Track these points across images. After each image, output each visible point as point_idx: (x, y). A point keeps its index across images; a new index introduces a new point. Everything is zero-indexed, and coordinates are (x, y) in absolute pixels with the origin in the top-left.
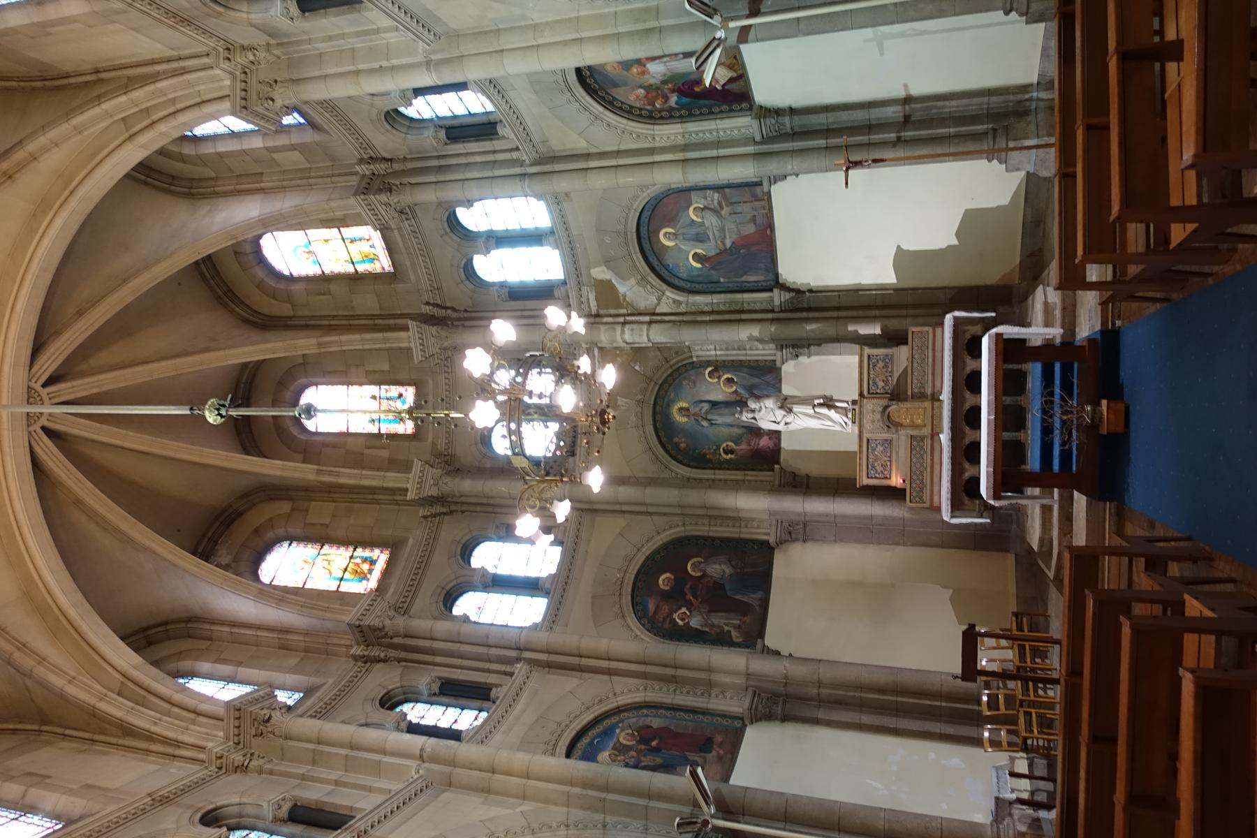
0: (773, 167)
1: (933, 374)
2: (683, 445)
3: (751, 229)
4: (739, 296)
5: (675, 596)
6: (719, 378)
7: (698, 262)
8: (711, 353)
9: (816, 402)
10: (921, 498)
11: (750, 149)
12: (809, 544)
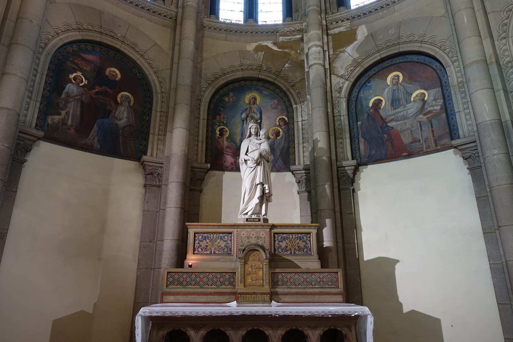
1: (297, 294)
2: (227, 99)
3: (406, 139)
4: (348, 135)
5: (98, 77)
6: (280, 126)
7: (374, 104)
9: (266, 186)
10: (172, 283)
12: (141, 190)
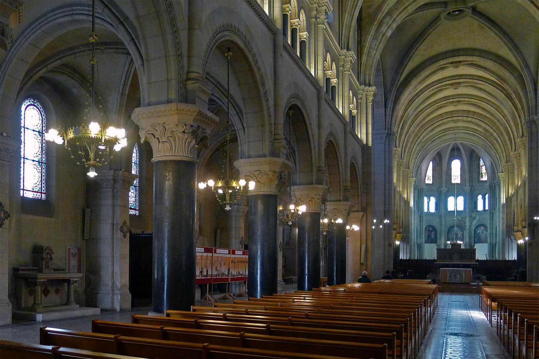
5: (429, 231)
8: (465, 233)
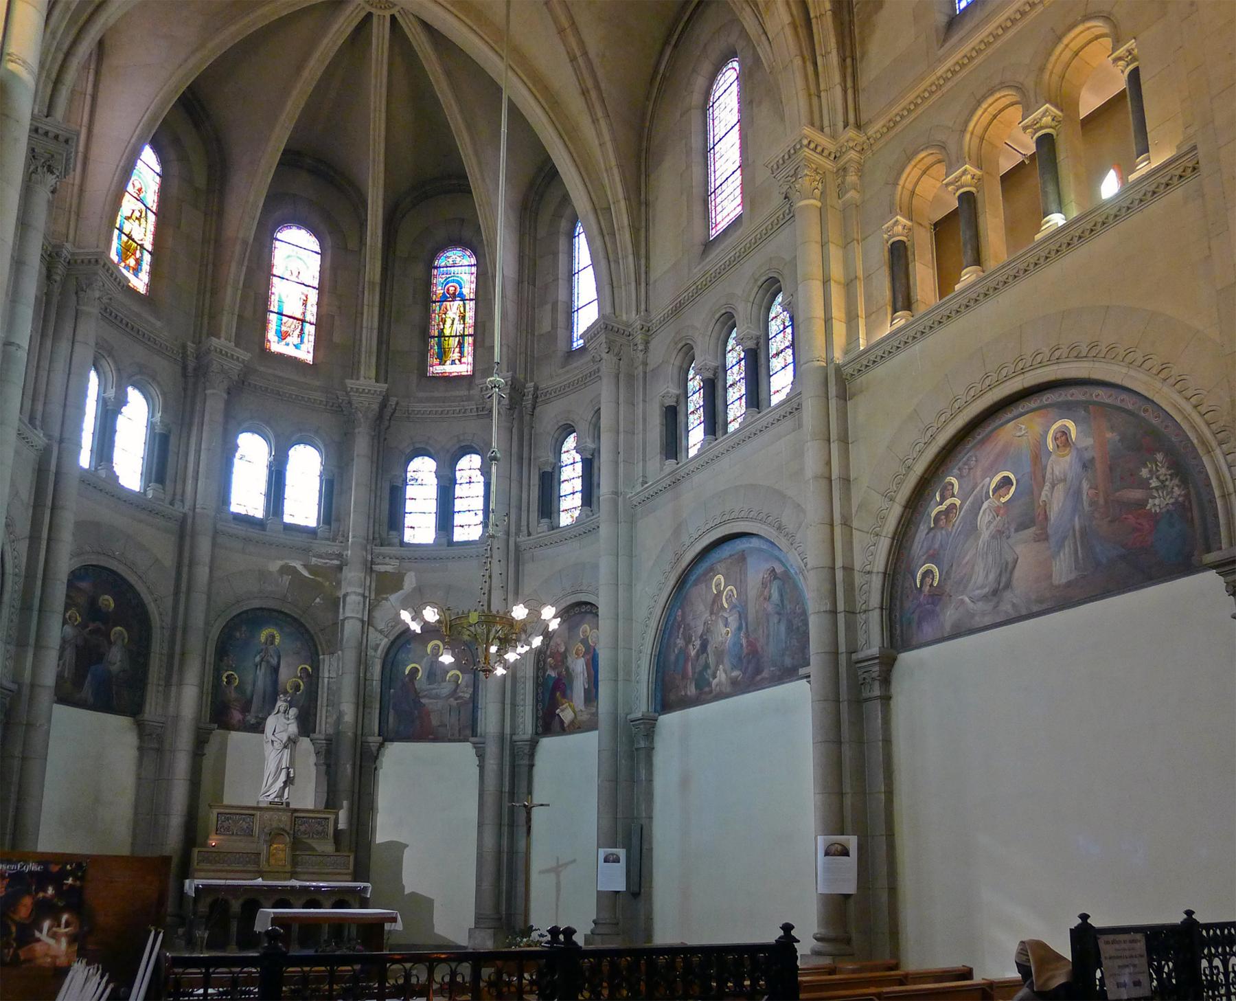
0: (492, 750)
11: (508, 731)
